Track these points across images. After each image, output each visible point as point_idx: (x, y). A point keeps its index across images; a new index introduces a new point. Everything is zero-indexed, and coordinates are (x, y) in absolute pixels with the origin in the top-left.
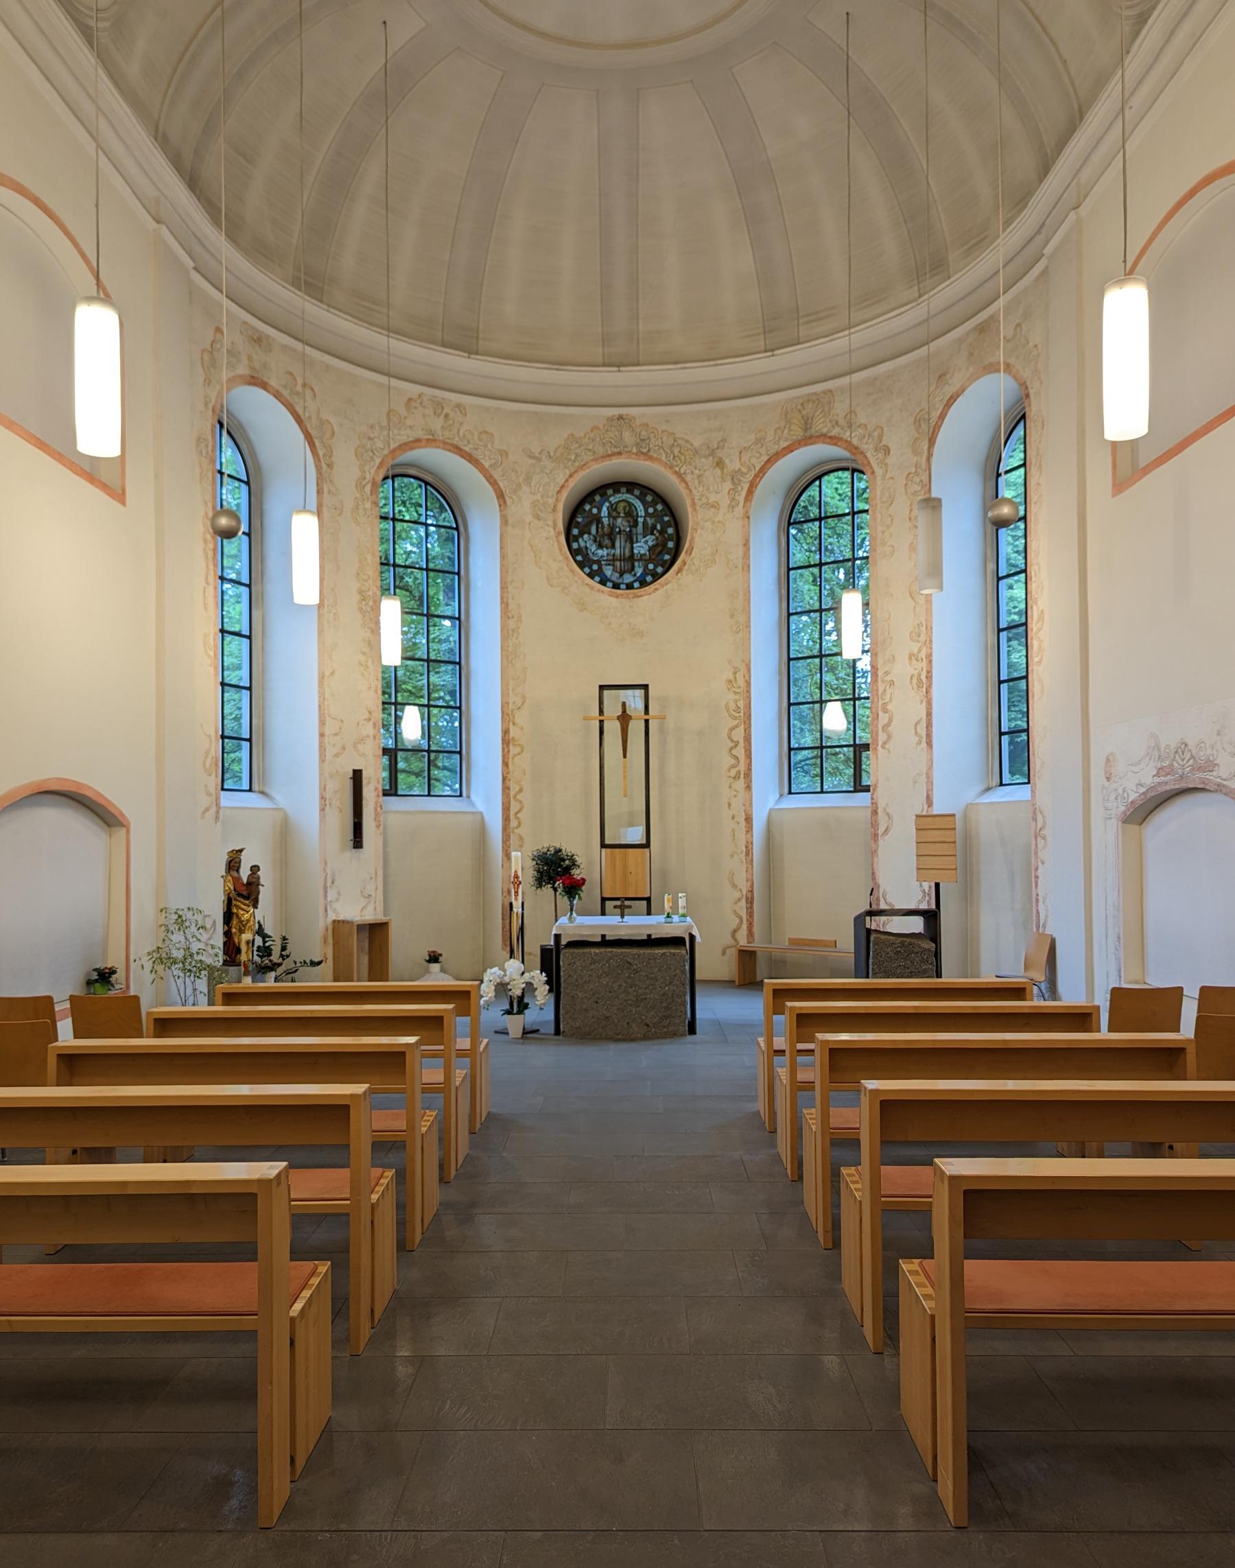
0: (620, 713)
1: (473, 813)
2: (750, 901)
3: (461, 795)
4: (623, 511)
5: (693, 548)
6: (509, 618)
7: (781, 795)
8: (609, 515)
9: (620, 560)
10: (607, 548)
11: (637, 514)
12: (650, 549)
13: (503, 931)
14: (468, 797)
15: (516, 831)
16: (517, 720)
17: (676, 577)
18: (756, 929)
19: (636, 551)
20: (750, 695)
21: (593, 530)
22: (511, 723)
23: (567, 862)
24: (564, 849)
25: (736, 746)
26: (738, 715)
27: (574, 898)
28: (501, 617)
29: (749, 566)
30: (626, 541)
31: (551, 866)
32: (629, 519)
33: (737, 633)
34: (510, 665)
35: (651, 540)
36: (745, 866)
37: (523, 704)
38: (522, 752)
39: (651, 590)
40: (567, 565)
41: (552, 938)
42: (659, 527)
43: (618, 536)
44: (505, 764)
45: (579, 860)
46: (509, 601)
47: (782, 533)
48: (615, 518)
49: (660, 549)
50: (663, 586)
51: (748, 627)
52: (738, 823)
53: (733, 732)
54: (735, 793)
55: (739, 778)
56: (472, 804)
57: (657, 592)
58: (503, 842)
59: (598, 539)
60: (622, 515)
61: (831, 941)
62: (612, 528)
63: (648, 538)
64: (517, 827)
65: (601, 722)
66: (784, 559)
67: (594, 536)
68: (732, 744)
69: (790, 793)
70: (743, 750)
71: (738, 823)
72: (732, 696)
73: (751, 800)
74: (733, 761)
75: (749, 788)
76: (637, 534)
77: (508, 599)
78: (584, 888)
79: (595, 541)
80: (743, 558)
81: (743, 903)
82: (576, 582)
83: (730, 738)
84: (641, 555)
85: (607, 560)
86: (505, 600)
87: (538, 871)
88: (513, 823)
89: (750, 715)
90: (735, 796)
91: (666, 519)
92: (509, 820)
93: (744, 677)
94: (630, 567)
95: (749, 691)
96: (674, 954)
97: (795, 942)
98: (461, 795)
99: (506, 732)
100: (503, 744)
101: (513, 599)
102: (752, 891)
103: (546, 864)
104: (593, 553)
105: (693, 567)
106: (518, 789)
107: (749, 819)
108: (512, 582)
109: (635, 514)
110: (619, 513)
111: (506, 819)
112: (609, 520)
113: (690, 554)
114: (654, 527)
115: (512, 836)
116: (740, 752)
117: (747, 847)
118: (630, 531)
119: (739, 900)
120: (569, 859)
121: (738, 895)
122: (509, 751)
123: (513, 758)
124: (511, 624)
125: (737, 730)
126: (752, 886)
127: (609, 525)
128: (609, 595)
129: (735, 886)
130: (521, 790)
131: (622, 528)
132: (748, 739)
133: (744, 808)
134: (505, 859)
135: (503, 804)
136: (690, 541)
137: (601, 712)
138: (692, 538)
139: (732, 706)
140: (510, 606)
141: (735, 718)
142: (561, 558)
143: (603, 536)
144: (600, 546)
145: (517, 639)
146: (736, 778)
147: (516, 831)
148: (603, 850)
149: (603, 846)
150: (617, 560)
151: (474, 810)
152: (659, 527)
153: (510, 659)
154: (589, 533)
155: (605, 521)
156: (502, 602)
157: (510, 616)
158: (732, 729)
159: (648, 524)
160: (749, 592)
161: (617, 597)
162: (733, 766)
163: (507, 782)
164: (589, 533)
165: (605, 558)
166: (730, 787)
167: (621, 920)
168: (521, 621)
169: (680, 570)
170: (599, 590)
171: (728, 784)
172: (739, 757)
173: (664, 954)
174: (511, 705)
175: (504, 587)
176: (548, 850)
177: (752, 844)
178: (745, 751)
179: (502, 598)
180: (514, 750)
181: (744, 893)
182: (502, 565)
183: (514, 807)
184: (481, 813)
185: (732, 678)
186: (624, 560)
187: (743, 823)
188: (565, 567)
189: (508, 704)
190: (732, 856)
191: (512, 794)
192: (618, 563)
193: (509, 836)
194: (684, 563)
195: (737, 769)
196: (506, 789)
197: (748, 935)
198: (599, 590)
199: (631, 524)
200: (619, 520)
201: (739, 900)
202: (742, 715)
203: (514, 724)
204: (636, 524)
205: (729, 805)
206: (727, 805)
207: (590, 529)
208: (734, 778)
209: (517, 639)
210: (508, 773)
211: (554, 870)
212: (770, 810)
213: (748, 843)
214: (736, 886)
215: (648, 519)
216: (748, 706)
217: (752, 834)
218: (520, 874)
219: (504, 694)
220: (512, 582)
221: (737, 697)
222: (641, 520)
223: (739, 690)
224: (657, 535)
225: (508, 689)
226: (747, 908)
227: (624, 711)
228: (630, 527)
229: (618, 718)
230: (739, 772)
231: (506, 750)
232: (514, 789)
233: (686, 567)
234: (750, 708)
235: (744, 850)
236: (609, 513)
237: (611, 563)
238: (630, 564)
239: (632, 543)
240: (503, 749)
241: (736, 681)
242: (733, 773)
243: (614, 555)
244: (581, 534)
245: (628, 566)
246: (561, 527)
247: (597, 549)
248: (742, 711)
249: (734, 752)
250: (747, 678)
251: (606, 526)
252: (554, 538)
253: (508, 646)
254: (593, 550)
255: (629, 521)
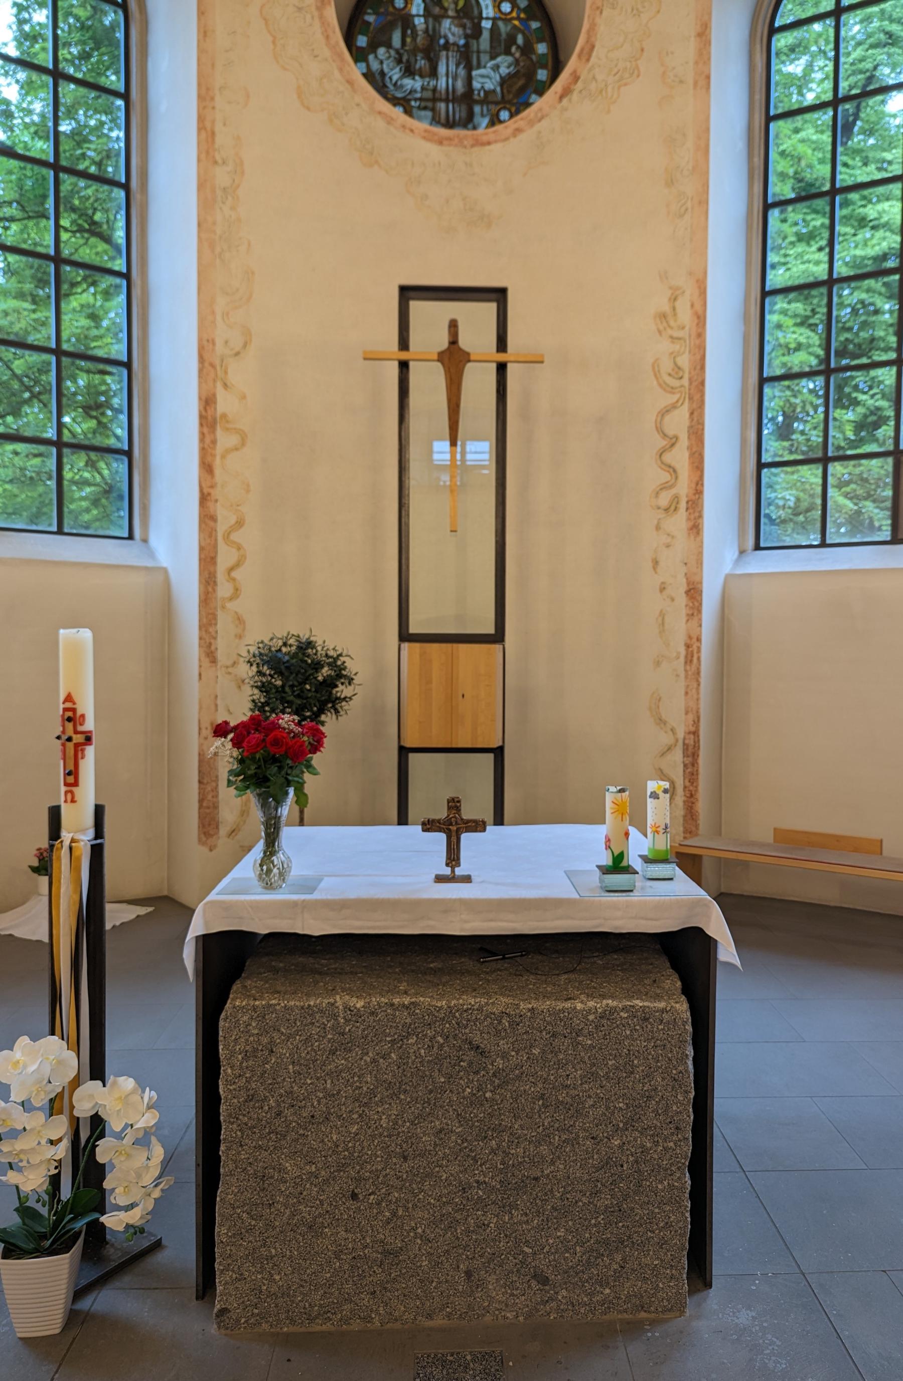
0: (444, 344)
1: (147, 569)
2: (691, 753)
3: (131, 537)
4: (452, 6)
5: (593, 47)
6: (216, 162)
7: (742, 552)
8: (427, 13)
9: (447, 101)
10: (422, 76)
11: (481, 13)
12: (503, 82)
13: (201, 807)
14: (145, 541)
15: (229, 605)
16: (234, 377)
17: (559, 106)
18: (702, 806)
19: (476, 85)
20: (704, 341)
21: (396, 39)
22: (219, 385)
23: (325, 671)
24: (320, 642)
25: (673, 445)
26: (676, 383)
27: (279, 802)
28: (199, 160)
29: (708, 77)
30: (457, 65)
31: (287, 679)
32: (465, 21)
33: (681, 216)
34: (218, 261)
35: (505, 64)
36: (682, 684)
37: (245, 345)
38: (243, 444)
39: (509, 131)
40: (341, 70)
41: (189, 955)
42: (520, 40)
43: (444, 53)
44: (207, 467)
45: (352, 666)
46: (217, 130)
47: (758, 46)
48: (438, 19)
49: (521, 82)
50: (531, 123)
51: (703, 202)
52: (673, 600)
53: (667, 418)
54: (669, 540)
55: (676, 509)
56: (152, 555)
57: (522, 137)
58: (200, 628)
59: (405, 58)
60: (451, 13)
61: (871, 841)
62: (432, 36)
63: (499, 59)
64: (231, 599)
65: (404, 366)
66: (759, 97)
67: (397, 51)
68: (664, 443)
69: (757, 547)
70: (687, 454)
71: (673, 600)
72: (664, 346)
73: (700, 553)
74: (665, 477)
75: (696, 528)
76: (478, 52)
77: (213, 122)
78: (316, 759)
79: (399, 61)
80: (696, 63)
81: (678, 756)
82: (358, 105)
83: (660, 430)
84: (487, 93)
85: (421, 99)
86: (208, 125)
87: (263, 688)
88: (223, 589)
89: (703, 383)
90: (668, 546)
91: (535, 25)
92: (215, 583)
93: (692, 306)
94: (464, 115)
95: (701, 335)
96: (646, 1017)
97: (784, 837)
98: (131, 537)
99: (207, 402)
100: (201, 425)
101: (225, 124)
102: (695, 733)
103: (281, 673)
104: (395, 84)
105: (593, 86)
106: (233, 520)
107: (694, 592)
108: (221, 89)
109: (476, 12)
110: (446, 10)
111: (208, 580)
112: (426, 22)
113: (588, 60)
114: (511, 40)
115: (220, 614)
116: (680, 457)
117: (688, 646)
118: (466, 45)
119: (669, 749)
120: (329, 664)
121: (666, 739)
122: (214, 442)
123: (223, 457)
124: (222, 176)
125: (676, 412)
126: (697, 722)
127: (426, 31)
128: (424, 138)
129: (661, 722)
130: (240, 524)
131: (452, 39)
132: (697, 433)
133: (684, 569)
134: (206, 662)
135: (201, 549)
136: (588, 32)
137: (404, 344)
138: (593, 27)
139: (666, 366)
140: (219, 140)
141: (672, 390)
142: (327, 53)
143: (414, 51)
144: (409, 72)
145: (233, 208)
146: (671, 509)
147: (229, 605)
148: (405, 646)
149: (405, 636)
150: (441, 100)
151: (150, 564)
152: (520, 40)
153: (218, 250)
154: (389, 45)
155: (419, 22)
156: (201, 127)
157: (218, 158)
158: (665, 412)
159: (500, 34)
160: (708, 130)
161: (440, 143)
162: (665, 487)
163: (210, 504)
164: (389, 45)
165: (418, 95)
166: (658, 528)
167: (447, 871)
168: (243, 173)
169: (566, 92)
170: (404, 127)
171: (656, 522)
172: (678, 467)
173: (608, 1014)
174: (219, 348)
175: (205, 96)
176: (285, 644)
177: (699, 640)
178: (692, 455)
179: (201, 119)
180: (224, 440)
181: (681, 735)
182: (201, 51)
183: (225, 557)
184: (165, 571)
185: (666, 308)
186: (453, 101)
187: (682, 600)
188: (336, 73)
189: (214, 344)
190: (658, 664)
191: (221, 528)
192: (442, 106)
193: (215, 617)
194: (576, 78)
195: (673, 491)
196: (207, 519)
197: (685, 816)
198: (404, 127)
199: (469, 32)
200: (446, 23)
201: (669, 749)
202: (685, 382)
203: (225, 386)
204: (477, 32)
205: (656, 563)
206: (650, 564)
207: (390, 39)
208: (667, 510)
209: (233, 208)
210: (212, 487)
211: (292, 686)
212: (728, 577)
213: (690, 638)
214: (665, 723)
215: (501, 24)
216: (700, 365)
217: (700, 619)
218: (87, 706)
219: (205, 322)
220: (221, 89)
221: (677, 347)
222: (486, 25)
223: (680, 334)
224: (517, 55)
225: (213, 313)
226: (685, 766)
227: (454, 342)
228: (466, 37)
229: (442, 357)
230: (676, 498)
231: (208, 440)
232: (225, 519)
233: (580, 85)
234: (703, 368)
235: (682, 650)
236: (426, 9)
237: (430, 104)
238: (464, 108)
239: (469, 68)
240: (202, 439)
241: (675, 315)
242: (664, 499)
243: (435, 90)
244: (373, 47)
245: (460, 112)
246: (338, 37)
247: (401, 78)
248: (686, 376)
249: (667, 457)
250: (698, 307)
251: (420, 33)
252: (313, 9)
253: (214, 223)
254: (395, 78)
255: (464, 26)
